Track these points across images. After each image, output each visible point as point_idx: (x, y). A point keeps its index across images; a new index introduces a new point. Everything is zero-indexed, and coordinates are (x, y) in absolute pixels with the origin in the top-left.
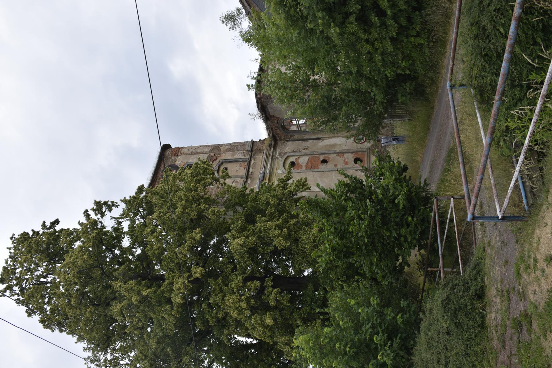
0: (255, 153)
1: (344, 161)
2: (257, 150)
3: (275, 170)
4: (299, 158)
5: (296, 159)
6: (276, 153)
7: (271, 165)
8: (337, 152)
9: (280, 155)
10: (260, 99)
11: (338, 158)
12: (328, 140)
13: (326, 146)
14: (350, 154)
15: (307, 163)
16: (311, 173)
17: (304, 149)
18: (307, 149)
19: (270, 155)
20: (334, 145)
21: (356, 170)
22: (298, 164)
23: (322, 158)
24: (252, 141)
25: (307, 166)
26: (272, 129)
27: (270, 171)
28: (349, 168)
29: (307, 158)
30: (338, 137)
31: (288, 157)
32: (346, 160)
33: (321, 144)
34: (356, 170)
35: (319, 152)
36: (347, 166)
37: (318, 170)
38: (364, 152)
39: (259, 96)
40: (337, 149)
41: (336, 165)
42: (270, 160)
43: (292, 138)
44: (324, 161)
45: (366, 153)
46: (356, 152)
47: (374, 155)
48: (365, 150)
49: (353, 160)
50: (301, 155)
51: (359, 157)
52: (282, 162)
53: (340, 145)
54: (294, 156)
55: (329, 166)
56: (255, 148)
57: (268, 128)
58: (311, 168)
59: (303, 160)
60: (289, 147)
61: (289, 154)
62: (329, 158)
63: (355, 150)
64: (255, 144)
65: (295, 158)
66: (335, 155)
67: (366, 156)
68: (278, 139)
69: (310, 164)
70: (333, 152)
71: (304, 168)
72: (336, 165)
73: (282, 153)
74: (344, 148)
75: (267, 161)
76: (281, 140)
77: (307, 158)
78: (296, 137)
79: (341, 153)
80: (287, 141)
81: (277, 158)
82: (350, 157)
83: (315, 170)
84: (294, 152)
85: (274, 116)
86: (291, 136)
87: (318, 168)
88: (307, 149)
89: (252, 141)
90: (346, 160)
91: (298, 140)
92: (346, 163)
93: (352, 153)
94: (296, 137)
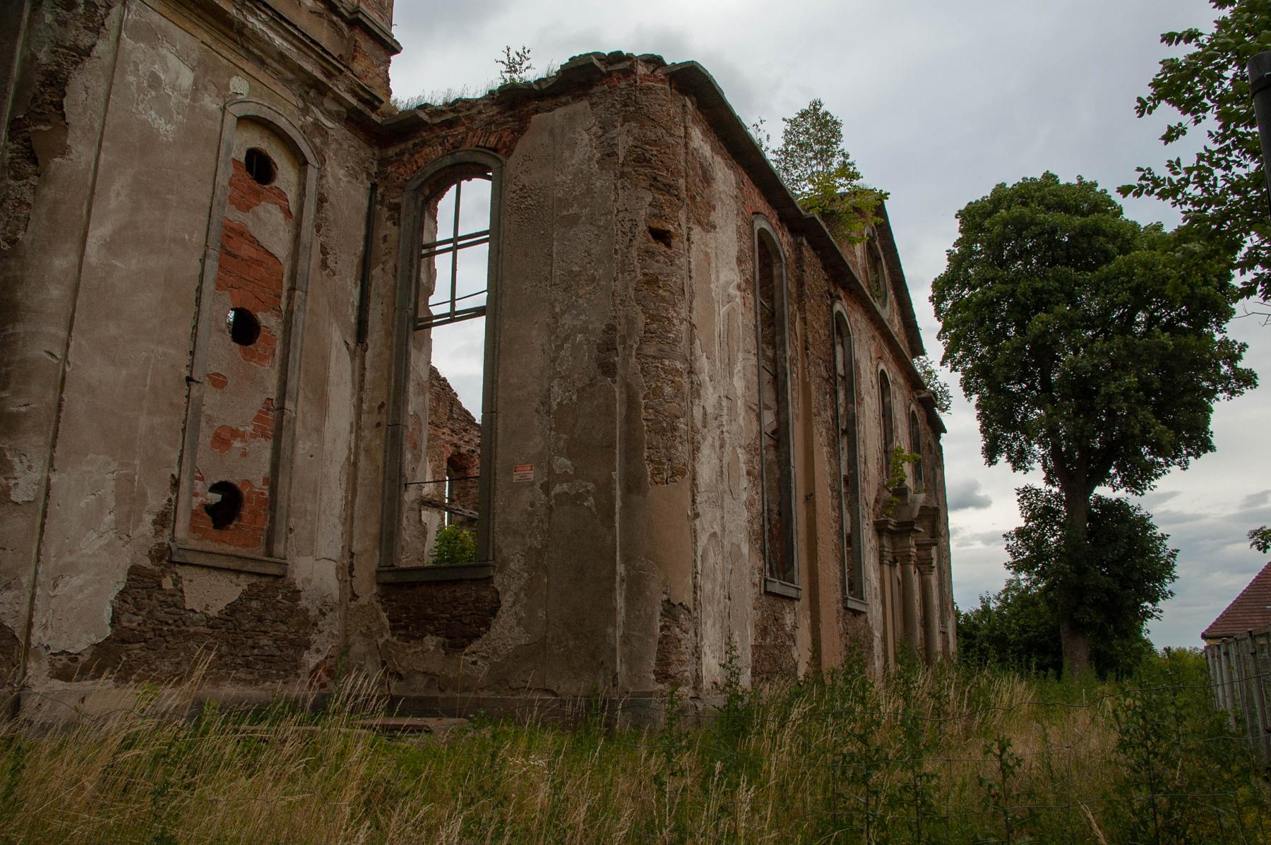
0: (339, 31)
1: (235, 433)
2: (356, 47)
3: (249, 67)
4: (288, 213)
5: (281, 195)
6: (329, 114)
7: (282, 58)
8: (289, 405)
9: (317, 125)
10: (629, 73)
11: (257, 402)
12: (347, 375)
13: (325, 359)
14: (266, 469)
15: (254, 242)
16: (198, 238)
17: (324, 251)
18: (324, 265)
19: (329, 75)
20: (321, 402)
21: (176, 484)
22: (258, 196)
23: (269, 321)
24: (392, 48)
25: (242, 233)
26: (450, 124)
27: (256, 37)
28: (194, 446)
29: (280, 246)
30: (357, 427)
31: (301, 162)
32: (237, 444)
33: (337, 339)
34: (176, 484)
35: (300, 318)
36: (205, 437)
37: (209, 285)
38: (270, 542)
39: (641, 70)
40: (300, 408)
41: (218, 382)
42: (308, 67)
43: (385, 213)
44: (245, 330)
45: (259, 552)
46: (272, 503)
47: (248, 595)
48: (279, 549)
49: (235, 480)
50: (298, 225)
51: (245, 512)
52: (282, 123)
53: (319, 430)
54: (302, 194)
55: (220, 350)
56: (365, 44)
57: (459, 110)
58: (227, 253)
59: (270, 227)
60: (343, 181)
61: (312, 173)
62: (262, 358)
63: (282, 500)
64: (381, 53)
65: (292, 196)
66: (273, 393)
67: (243, 552)
68: (391, 152)
69: (246, 251)
70: (292, 384)
71: (236, 216)
72: (218, 382)
73: (325, 143)
74: (303, 447)
75: (307, 44)
76: (383, 162)
77: (280, 246)
78: (387, 229)
79: (276, 422)
80: (374, 187)
81: (305, 111)
82: (249, 467)
83: (212, 265)
84: (322, 200)
85: (522, 131)
86: (396, 208)
87: (218, 287)
88: (324, 265)
89: (392, 48)
90: (237, 444)
91: (368, 238)
92: (222, 440)
93: (273, 481)
94: (387, 229)
